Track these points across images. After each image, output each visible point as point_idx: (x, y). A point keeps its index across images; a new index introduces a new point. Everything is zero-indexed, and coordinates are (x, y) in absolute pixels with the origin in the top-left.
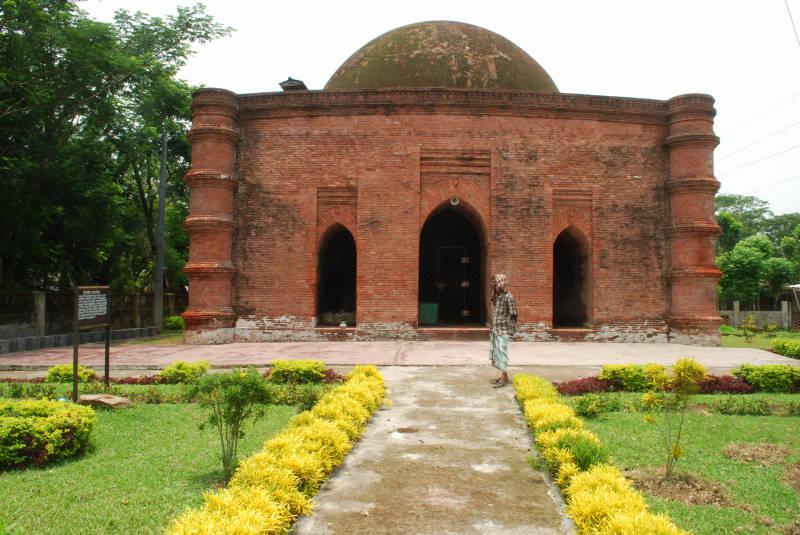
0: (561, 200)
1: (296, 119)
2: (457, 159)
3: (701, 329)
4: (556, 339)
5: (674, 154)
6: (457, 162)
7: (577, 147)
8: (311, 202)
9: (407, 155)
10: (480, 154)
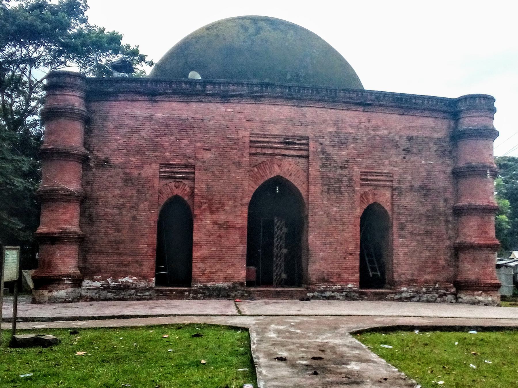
0: (367, 180)
1: (142, 103)
2: (281, 143)
3: (484, 291)
4: (363, 299)
5: (461, 144)
8: (154, 175)
9: (238, 139)
10: (301, 140)
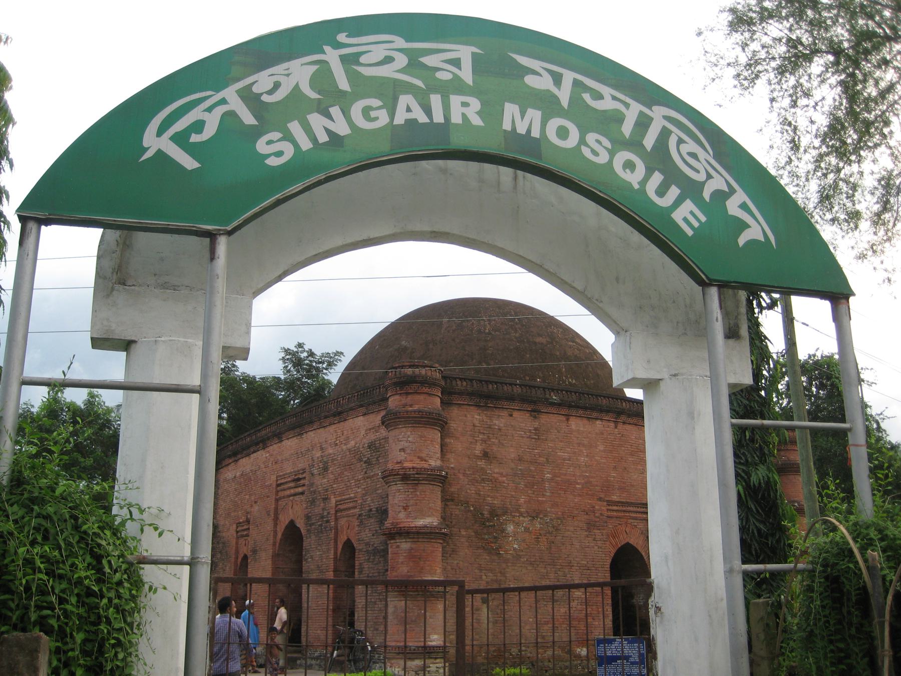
6: (292, 485)
7: (350, 450)
